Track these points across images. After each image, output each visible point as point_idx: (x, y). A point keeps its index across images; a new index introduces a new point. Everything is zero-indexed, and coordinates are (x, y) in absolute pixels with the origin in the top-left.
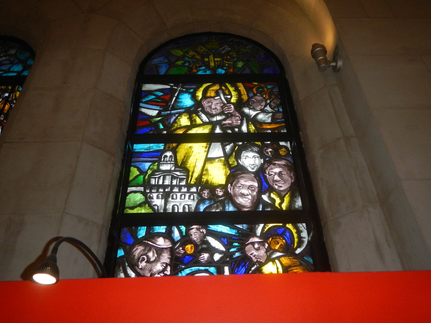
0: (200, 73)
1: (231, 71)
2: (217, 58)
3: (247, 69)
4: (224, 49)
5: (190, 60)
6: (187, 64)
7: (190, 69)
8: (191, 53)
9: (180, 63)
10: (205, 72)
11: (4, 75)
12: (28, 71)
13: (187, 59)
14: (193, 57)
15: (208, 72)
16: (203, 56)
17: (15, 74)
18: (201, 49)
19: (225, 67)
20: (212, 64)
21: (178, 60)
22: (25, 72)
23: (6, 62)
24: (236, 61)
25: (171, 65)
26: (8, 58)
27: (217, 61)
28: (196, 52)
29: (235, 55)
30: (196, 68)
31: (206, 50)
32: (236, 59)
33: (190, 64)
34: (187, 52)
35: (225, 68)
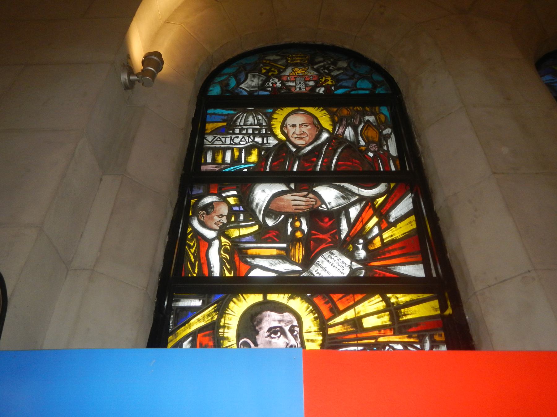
11: (353, 93)
12: (381, 88)
23: (344, 77)
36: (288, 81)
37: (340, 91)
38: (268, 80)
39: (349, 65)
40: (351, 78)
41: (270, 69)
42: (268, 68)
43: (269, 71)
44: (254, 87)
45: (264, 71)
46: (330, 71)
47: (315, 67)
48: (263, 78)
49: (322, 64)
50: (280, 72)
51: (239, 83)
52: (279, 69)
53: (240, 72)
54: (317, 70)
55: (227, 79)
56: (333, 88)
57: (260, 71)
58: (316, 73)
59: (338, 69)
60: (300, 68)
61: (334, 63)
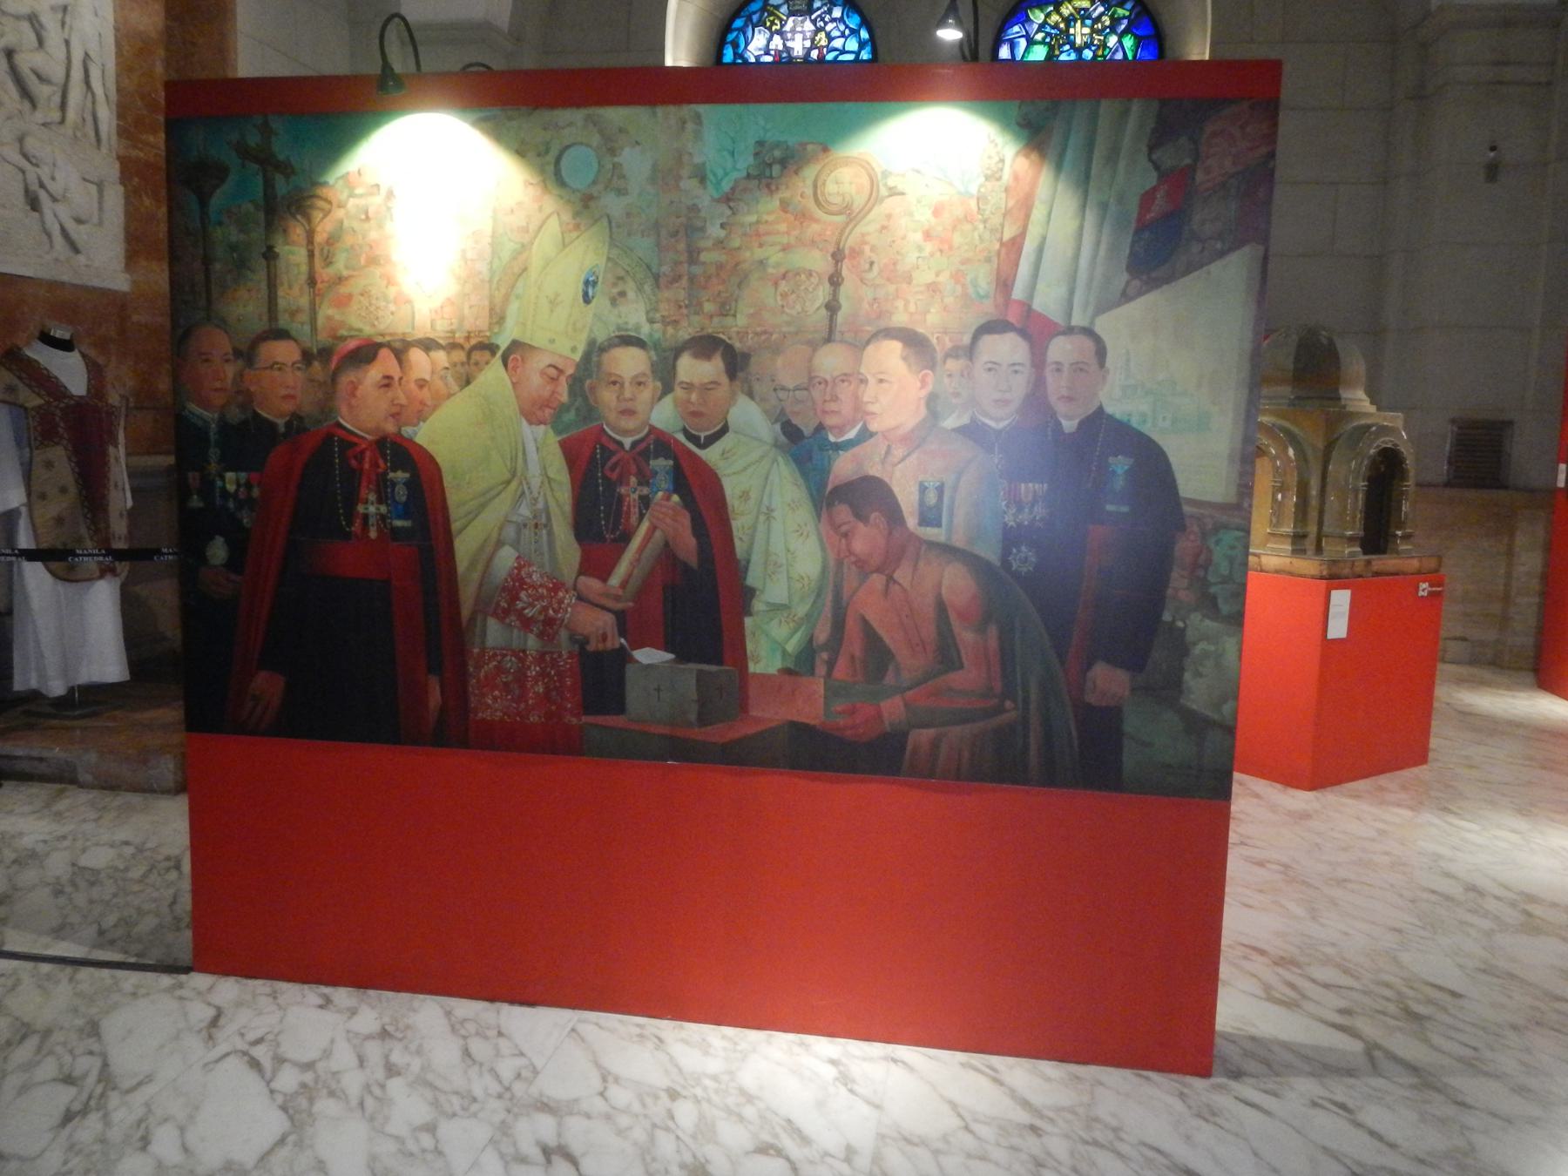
0: (1063, 57)
1: (1100, 53)
2: (1086, 26)
3: (1120, 49)
4: (1095, 9)
5: (1053, 31)
6: (1048, 40)
7: (1051, 48)
8: (1055, 18)
9: (1039, 37)
10: (1069, 55)
11: (841, 58)
13: (1048, 29)
14: (1056, 26)
15: (1073, 57)
16: (1069, 21)
17: (850, 57)
18: (1067, 8)
19: (1094, 46)
20: (1078, 41)
21: (1037, 33)
22: (863, 52)
23: (838, 34)
24: (1108, 33)
25: (1031, 42)
26: (835, 24)
27: (1085, 35)
28: (1060, 15)
29: (1108, 23)
30: (1061, 46)
31: (1073, 11)
32: (1108, 30)
33: (1052, 39)
34: (1048, 15)
35: (1093, 48)
36: (788, 40)
37: (830, 57)
38: (770, 40)
39: (842, 14)
40: (843, 35)
41: (774, 20)
42: (771, 18)
43: (773, 23)
44: (760, 49)
45: (768, 24)
46: (826, 23)
47: (813, 17)
48: (768, 34)
49: (819, 12)
50: (782, 26)
51: (747, 44)
52: (781, 20)
53: (748, 26)
54: (814, 22)
55: (737, 37)
56: (825, 50)
57: (764, 25)
58: (813, 28)
59: (834, 20)
60: (800, 18)
61: (830, 12)
